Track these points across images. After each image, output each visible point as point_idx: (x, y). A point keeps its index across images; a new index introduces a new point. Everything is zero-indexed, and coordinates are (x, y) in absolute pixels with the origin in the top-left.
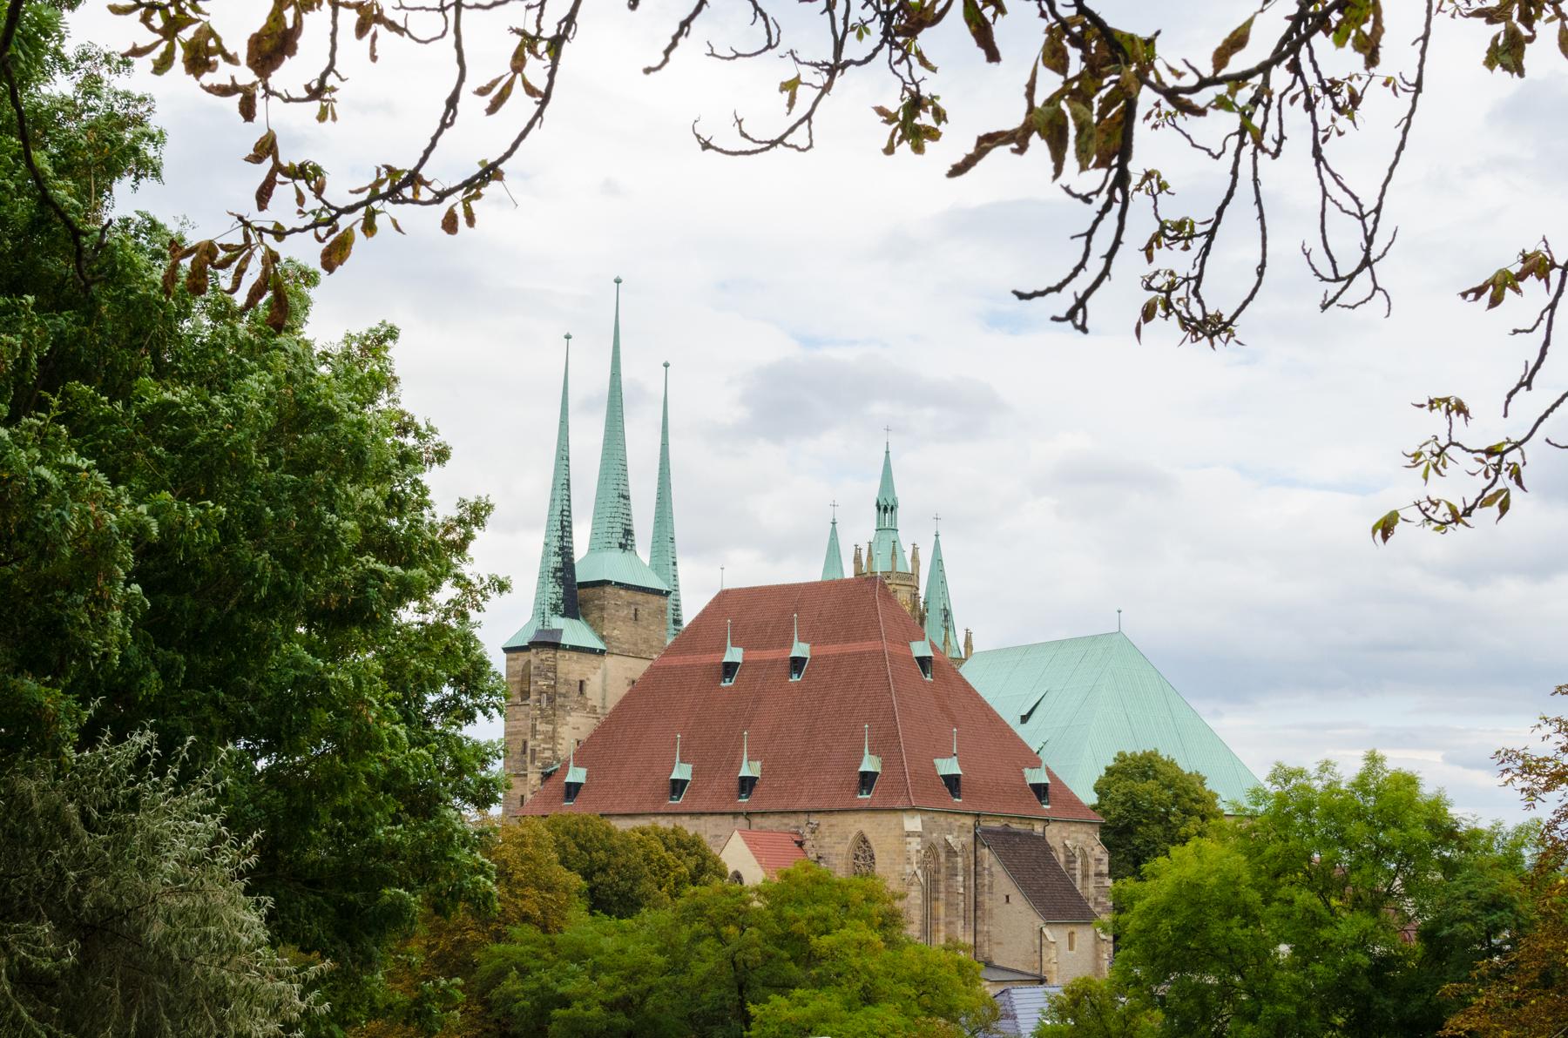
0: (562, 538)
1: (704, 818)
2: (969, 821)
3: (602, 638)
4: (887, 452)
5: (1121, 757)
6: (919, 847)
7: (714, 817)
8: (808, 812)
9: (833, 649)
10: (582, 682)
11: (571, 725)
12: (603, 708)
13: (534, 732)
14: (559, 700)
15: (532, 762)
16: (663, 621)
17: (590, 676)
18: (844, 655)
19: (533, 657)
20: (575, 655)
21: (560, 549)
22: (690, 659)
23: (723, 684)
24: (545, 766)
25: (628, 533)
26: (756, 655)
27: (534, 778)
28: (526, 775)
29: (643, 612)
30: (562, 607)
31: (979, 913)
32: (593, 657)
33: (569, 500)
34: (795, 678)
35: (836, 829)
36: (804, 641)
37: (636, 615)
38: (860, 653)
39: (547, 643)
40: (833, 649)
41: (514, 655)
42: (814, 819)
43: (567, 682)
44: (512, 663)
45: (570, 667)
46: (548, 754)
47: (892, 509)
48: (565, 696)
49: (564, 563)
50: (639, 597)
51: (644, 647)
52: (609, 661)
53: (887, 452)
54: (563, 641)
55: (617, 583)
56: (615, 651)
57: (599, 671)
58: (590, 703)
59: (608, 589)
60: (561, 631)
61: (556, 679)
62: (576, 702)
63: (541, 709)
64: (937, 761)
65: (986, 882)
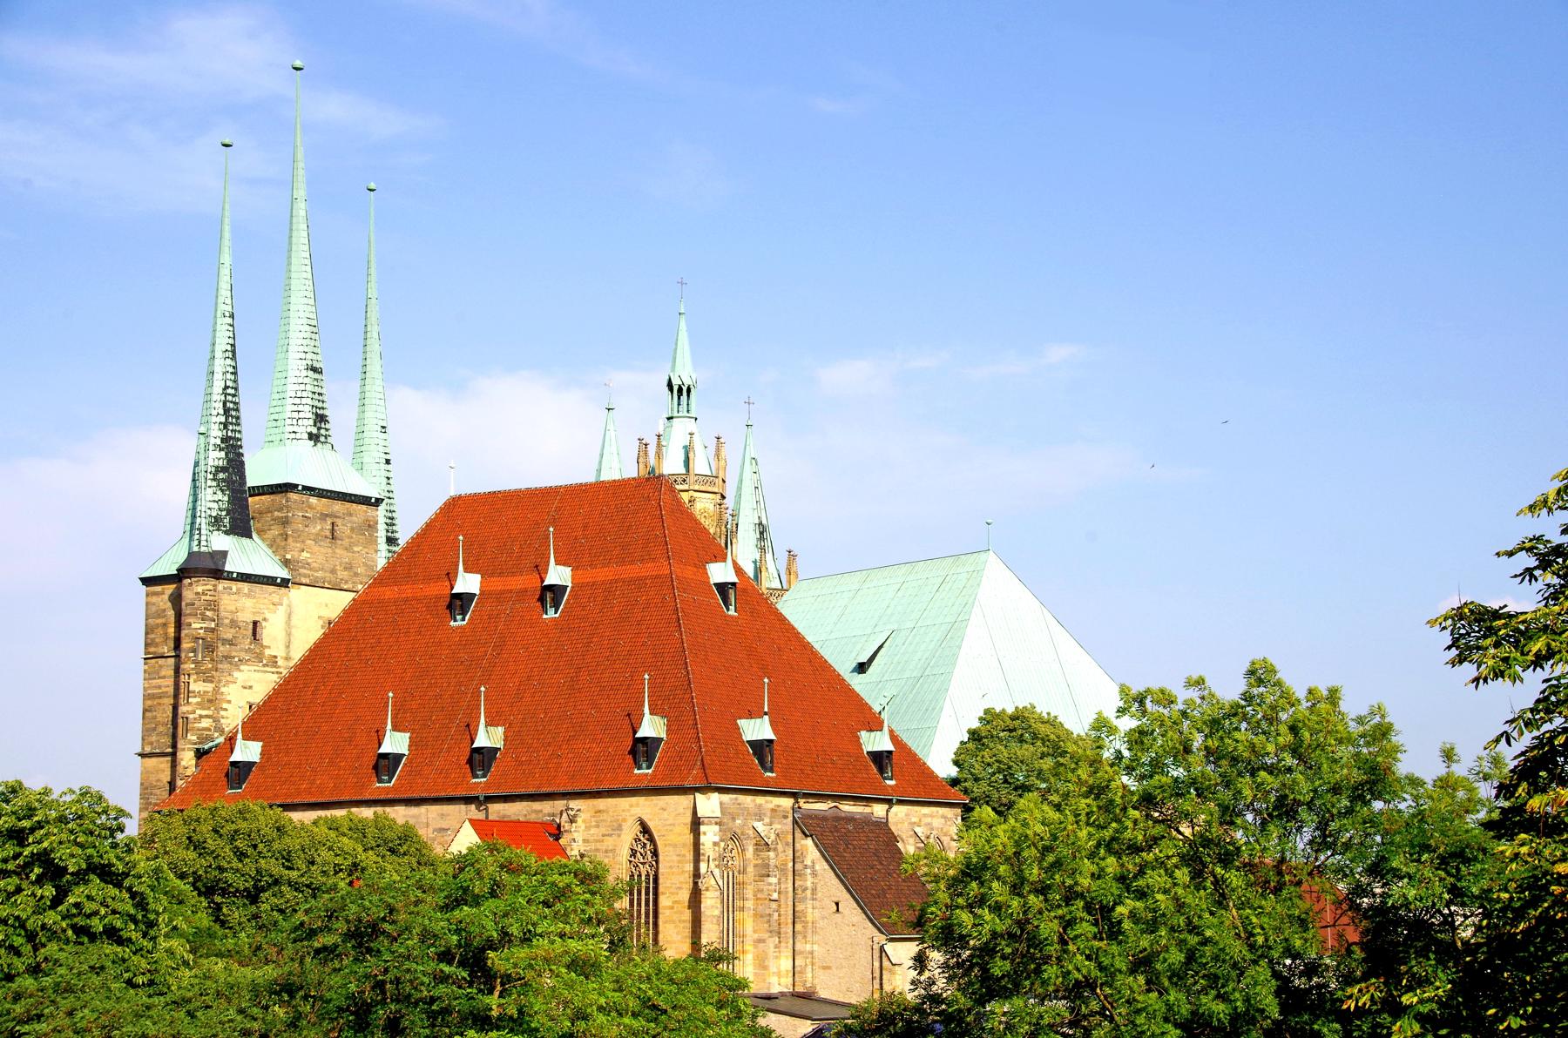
2: (787, 802)
3: (286, 563)
5: (989, 717)
6: (717, 839)
9: (602, 574)
10: (255, 623)
11: (240, 683)
12: (287, 658)
14: (223, 649)
16: (373, 541)
17: (268, 615)
20: (245, 587)
21: (223, 440)
22: (408, 591)
23: (452, 623)
24: (203, 740)
25: (320, 419)
29: (343, 529)
30: (227, 521)
31: (798, 927)
32: (272, 588)
33: (235, 373)
35: (604, 816)
36: (565, 564)
37: (333, 531)
38: (639, 579)
39: (208, 567)
40: (602, 574)
41: (158, 589)
42: (575, 804)
43: (234, 624)
44: (154, 599)
45: (240, 603)
46: (206, 723)
48: (231, 643)
49: (229, 461)
50: (338, 507)
51: (343, 574)
52: (296, 594)
54: (227, 568)
55: (305, 488)
56: (304, 580)
57: (282, 610)
58: (267, 652)
59: (293, 496)
60: (224, 554)
61: (218, 620)
63: (194, 662)
64: (742, 723)
65: (809, 884)
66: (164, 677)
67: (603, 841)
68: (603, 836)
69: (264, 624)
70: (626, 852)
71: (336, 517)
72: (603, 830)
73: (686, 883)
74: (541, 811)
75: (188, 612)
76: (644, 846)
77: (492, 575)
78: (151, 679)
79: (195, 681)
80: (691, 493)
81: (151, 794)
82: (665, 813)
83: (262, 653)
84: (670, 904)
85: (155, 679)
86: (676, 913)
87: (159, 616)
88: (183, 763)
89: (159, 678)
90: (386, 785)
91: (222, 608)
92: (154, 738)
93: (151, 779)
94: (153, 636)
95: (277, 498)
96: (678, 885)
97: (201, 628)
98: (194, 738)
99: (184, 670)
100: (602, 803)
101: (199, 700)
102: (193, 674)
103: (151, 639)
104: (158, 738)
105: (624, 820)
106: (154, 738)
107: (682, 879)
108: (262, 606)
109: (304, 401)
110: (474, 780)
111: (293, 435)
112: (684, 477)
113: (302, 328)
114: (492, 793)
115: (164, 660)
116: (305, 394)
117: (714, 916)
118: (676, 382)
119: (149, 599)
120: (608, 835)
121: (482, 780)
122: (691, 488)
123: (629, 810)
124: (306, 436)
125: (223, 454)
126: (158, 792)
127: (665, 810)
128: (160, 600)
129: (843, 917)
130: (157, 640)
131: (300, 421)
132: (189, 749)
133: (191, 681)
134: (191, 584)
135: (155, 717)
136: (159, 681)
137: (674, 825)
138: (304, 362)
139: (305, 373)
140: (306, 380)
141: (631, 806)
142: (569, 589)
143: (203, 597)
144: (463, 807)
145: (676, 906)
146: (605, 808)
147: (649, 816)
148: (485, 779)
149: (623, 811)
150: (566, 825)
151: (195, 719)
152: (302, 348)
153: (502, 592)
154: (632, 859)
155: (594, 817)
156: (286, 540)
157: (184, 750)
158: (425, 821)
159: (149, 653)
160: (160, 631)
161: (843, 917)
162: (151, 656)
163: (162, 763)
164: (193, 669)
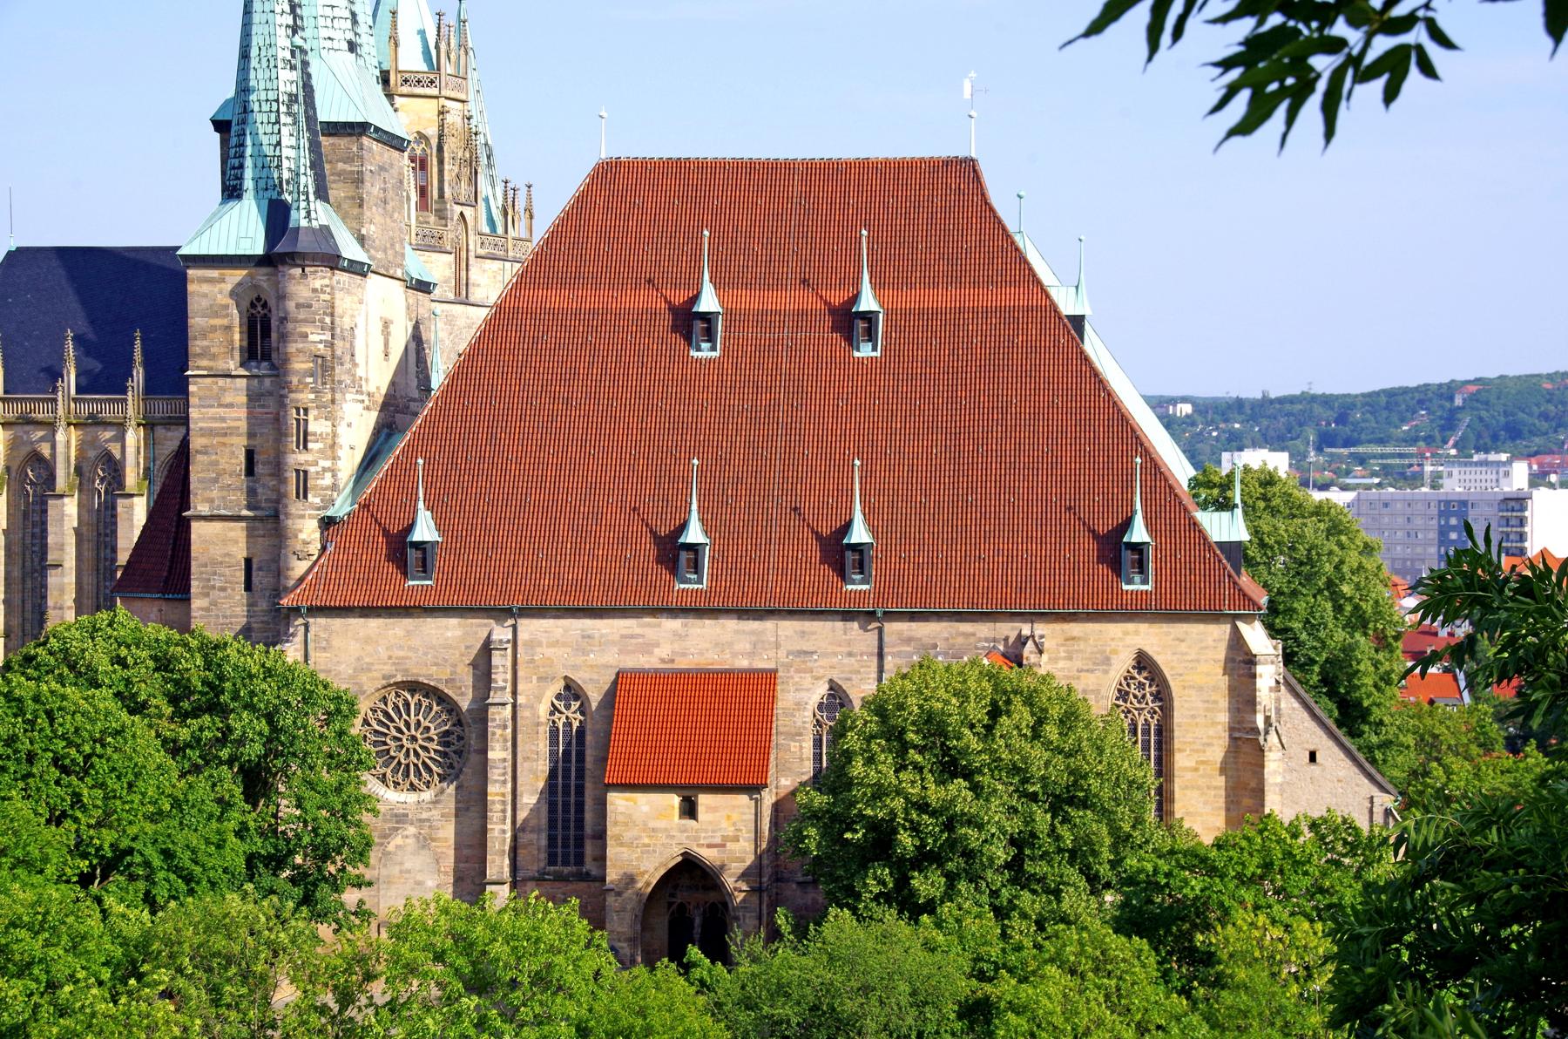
0: (295, 29)
3: (362, 240)
14: (338, 369)
22: (591, 300)
23: (694, 353)
26: (748, 300)
46: (327, 480)
55: (377, 129)
57: (363, 306)
59: (365, 141)
61: (333, 329)
62: (349, 372)
66: (230, 405)
67: (1078, 678)
68: (1082, 671)
69: (356, 331)
70: (1112, 693)
71: (386, 170)
72: (1079, 664)
73: (1220, 738)
74: (974, 635)
75: (301, 317)
76: (1141, 686)
78: (204, 407)
79: (315, 419)
80: (442, 101)
81: (215, 574)
82: (1183, 644)
83: (354, 375)
84: (1194, 764)
85: (212, 406)
86: (1202, 776)
87: (216, 315)
88: (302, 536)
89: (220, 406)
90: (696, 586)
91: (338, 311)
92: (215, 493)
93: (212, 551)
94: (205, 343)
95: (342, 142)
96: (1205, 740)
97: (321, 342)
98: (317, 500)
99: (298, 401)
100: (1075, 629)
102: (313, 408)
103: (202, 348)
104: (225, 493)
105: (1115, 652)
106: (215, 493)
108: (354, 306)
110: (850, 587)
111: (328, 44)
112: (432, 77)
115: (228, 380)
117: (1276, 784)
120: (1087, 671)
121: (865, 587)
122: (443, 93)
123: (1121, 639)
124: (345, 46)
125: (294, 75)
127: (1183, 641)
128: (216, 290)
129: (1323, 770)
131: (336, 21)
132: (311, 517)
133: (311, 417)
135: (216, 463)
137: (1198, 661)
141: (1126, 633)
142: (881, 316)
143: (323, 297)
144: (839, 624)
145: (1202, 767)
146: (1081, 634)
147: (1155, 648)
148: (867, 587)
149: (1113, 639)
150: (1032, 656)
151: (317, 473)
153: (765, 313)
154: (1120, 702)
155: (1063, 645)
156: (361, 206)
157: (302, 517)
158: (774, 639)
159: (198, 368)
160: (219, 337)
161: (1323, 770)
162: (205, 373)
163: (231, 529)
164: (312, 401)
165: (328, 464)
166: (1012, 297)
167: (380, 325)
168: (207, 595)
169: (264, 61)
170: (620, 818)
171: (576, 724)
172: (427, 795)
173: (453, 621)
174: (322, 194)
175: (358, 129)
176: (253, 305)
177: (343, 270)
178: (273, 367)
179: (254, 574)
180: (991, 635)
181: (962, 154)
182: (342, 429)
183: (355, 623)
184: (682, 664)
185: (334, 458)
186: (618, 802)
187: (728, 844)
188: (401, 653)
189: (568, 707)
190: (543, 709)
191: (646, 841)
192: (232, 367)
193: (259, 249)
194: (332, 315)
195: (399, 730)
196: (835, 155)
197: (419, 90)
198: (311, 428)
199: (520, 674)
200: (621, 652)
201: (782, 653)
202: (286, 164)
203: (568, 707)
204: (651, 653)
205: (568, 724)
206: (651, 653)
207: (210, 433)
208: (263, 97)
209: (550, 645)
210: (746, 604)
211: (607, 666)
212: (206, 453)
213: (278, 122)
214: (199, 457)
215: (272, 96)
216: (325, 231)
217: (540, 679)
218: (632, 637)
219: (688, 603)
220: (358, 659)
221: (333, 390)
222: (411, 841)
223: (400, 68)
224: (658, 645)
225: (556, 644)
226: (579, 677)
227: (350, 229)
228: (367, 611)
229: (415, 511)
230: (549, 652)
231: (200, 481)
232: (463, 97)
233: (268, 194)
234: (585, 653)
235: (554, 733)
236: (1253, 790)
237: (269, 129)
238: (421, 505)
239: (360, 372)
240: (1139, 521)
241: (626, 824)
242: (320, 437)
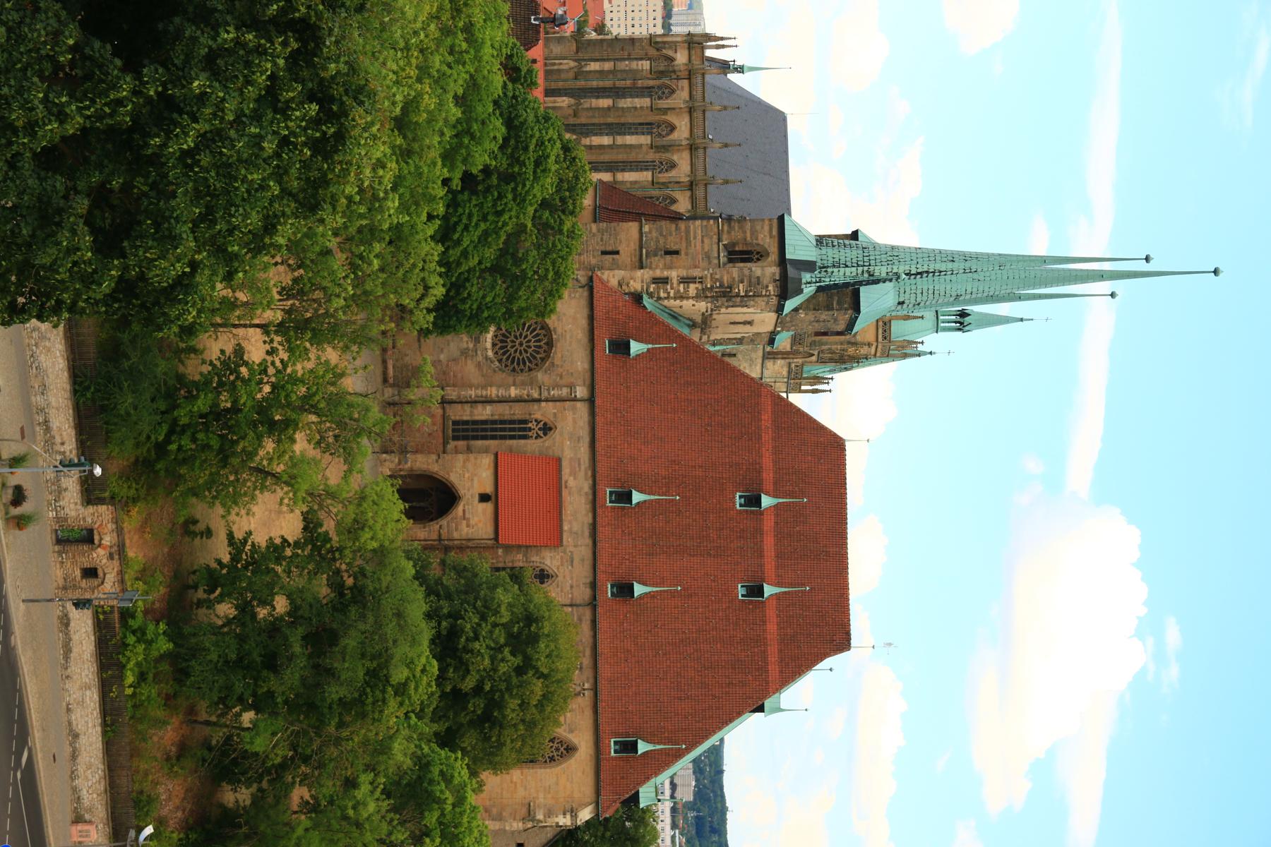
1: (589, 541)
3: (796, 310)
4: (1022, 320)
7: (590, 555)
8: (595, 690)
9: (772, 628)
13: (686, 281)
14: (725, 299)
15: (656, 281)
18: (765, 644)
19: (767, 271)
22: (767, 437)
26: (769, 523)
27: (638, 280)
28: (641, 267)
34: (741, 591)
40: (772, 628)
46: (662, 295)
47: (959, 329)
53: (1022, 320)
55: (857, 318)
61: (746, 296)
63: (712, 287)
66: (703, 242)
77: (777, 515)
79: (697, 288)
80: (875, 344)
84: (514, 780)
89: (702, 236)
91: (757, 299)
92: (654, 234)
100: (588, 713)
101: (682, 289)
107: (532, 790)
109: (931, 296)
111: (902, 291)
113: (992, 289)
114: (599, 610)
116: (936, 295)
118: (967, 320)
119: (767, 222)
124: (901, 300)
126: (612, 242)
130: (733, 233)
132: (642, 287)
133: (697, 285)
134: (775, 281)
135: (671, 235)
136: (699, 237)
137: (572, 782)
138: (963, 293)
139: (954, 294)
140: (948, 295)
152: (975, 290)
156: (815, 309)
165: (672, 295)
166: (774, 671)
167: (749, 320)
168: (599, 231)
169: (891, 258)
170: (479, 461)
171: (530, 434)
172: (490, 353)
173: (587, 366)
174: (820, 289)
175: (856, 307)
176: (758, 253)
177: (779, 302)
178: (725, 264)
179: (611, 256)
180: (584, 667)
181: (853, 642)
182: (691, 302)
183: (585, 312)
184: (565, 493)
185: (675, 298)
186: (487, 461)
187: (465, 522)
188: (568, 337)
189: (540, 429)
190: (538, 416)
191: (467, 475)
192: (725, 242)
193: (788, 256)
194: (754, 296)
195: (526, 337)
196: (850, 571)
197: (880, 331)
198: (692, 286)
199: (558, 403)
200: (571, 459)
201: (571, 549)
202: (836, 270)
203: (540, 429)
204: (570, 475)
205: (530, 429)
206: (570, 475)
207: (687, 231)
208: (872, 258)
209: (574, 419)
210: (599, 529)
211: (563, 451)
212: (676, 229)
213: (858, 266)
214: (674, 226)
215: (872, 262)
216: (801, 291)
217: (555, 414)
218: (579, 464)
219: (599, 495)
220: (564, 314)
221: (712, 297)
222: (465, 345)
223: (893, 322)
224: (575, 479)
225: (575, 422)
226: (555, 436)
227: (802, 304)
228: (591, 318)
229: (646, 343)
230: (570, 419)
231: (661, 226)
232: (878, 355)
233: (819, 261)
234: (570, 439)
235: (525, 422)
236: (501, 814)
237: (854, 261)
238: (650, 346)
239: (723, 310)
240: (650, 747)
241: (475, 464)
242: (686, 290)
